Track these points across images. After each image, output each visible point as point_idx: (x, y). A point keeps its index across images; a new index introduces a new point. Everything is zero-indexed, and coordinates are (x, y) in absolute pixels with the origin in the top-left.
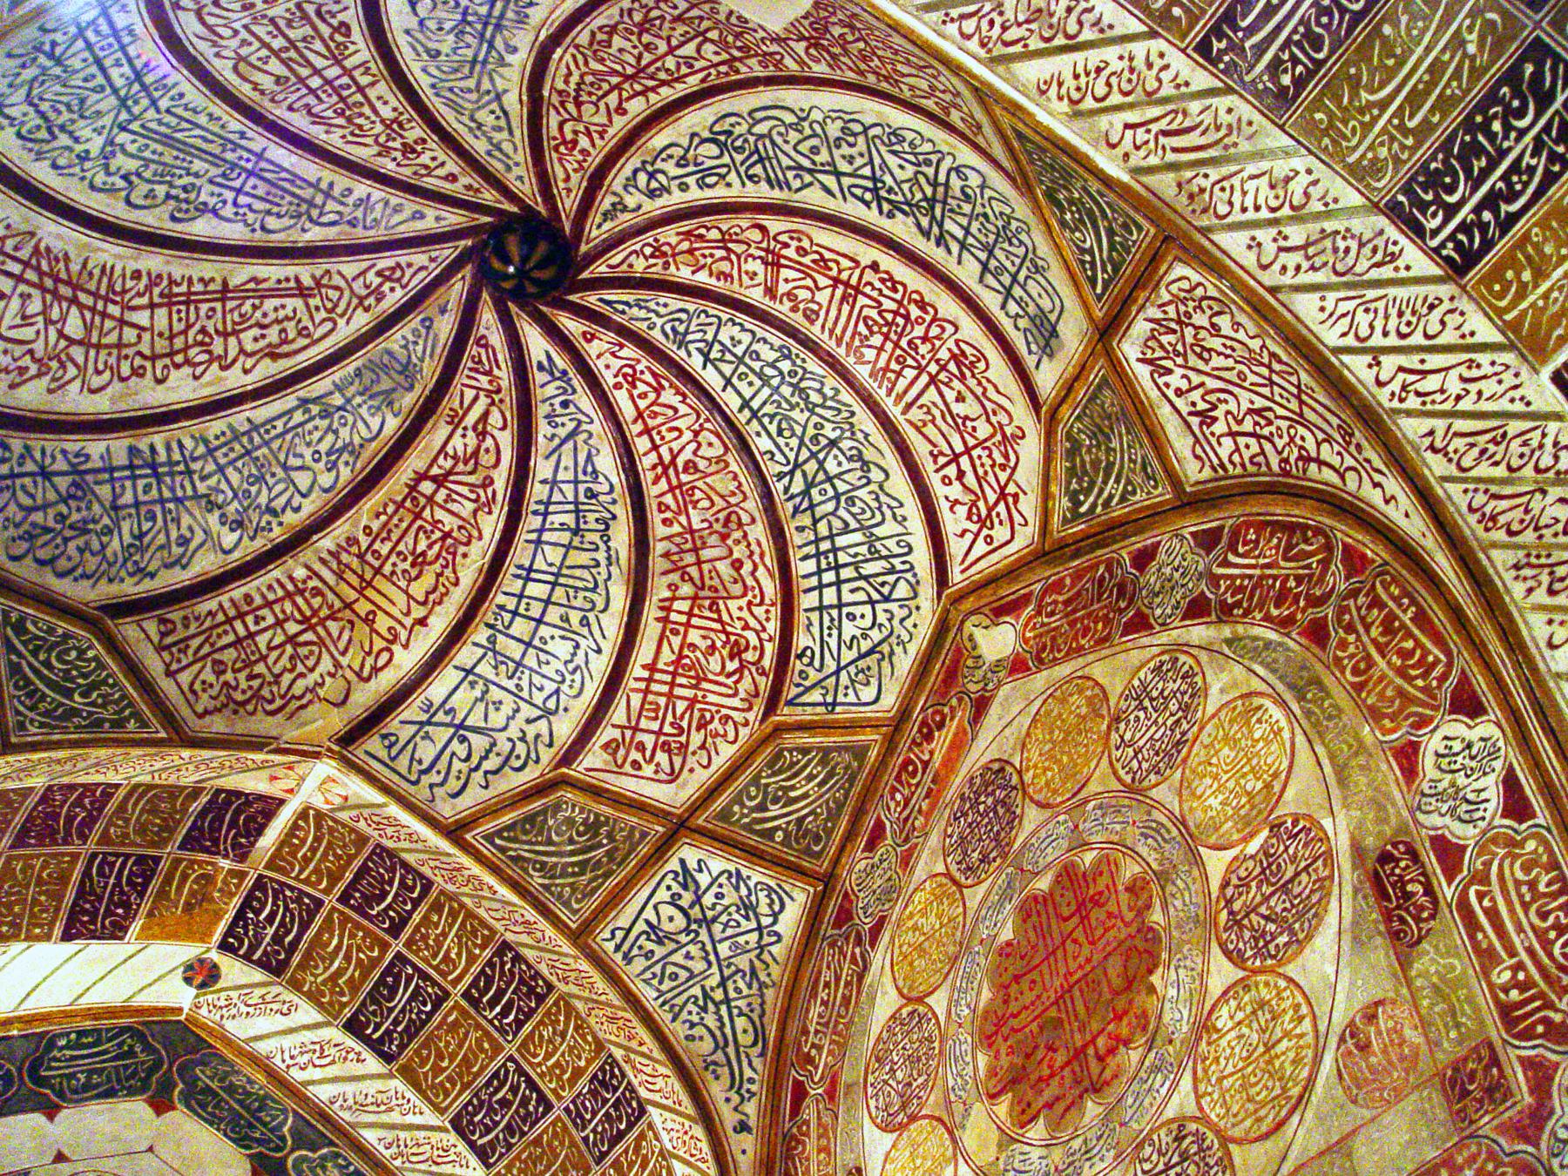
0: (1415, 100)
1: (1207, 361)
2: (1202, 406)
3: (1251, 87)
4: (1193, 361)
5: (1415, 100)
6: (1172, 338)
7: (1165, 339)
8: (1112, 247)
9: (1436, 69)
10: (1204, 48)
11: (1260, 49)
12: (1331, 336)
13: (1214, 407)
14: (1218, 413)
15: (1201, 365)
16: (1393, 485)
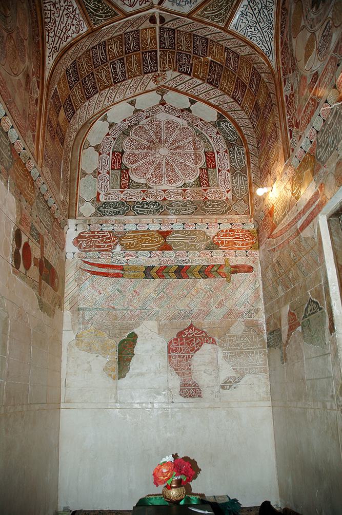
0: (82, 65)
1: (66, 14)
2: (57, 6)
3: (96, 46)
4: (66, 12)
5: (82, 65)
6: (71, 10)
7: (71, 8)
8: (91, 12)
9: (83, 68)
10: (105, 42)
11: (99, 47)
12: (69, 52)
13: (56, 9)
14: (54, 10)
15: (65, 13)
16: (52, 62)
